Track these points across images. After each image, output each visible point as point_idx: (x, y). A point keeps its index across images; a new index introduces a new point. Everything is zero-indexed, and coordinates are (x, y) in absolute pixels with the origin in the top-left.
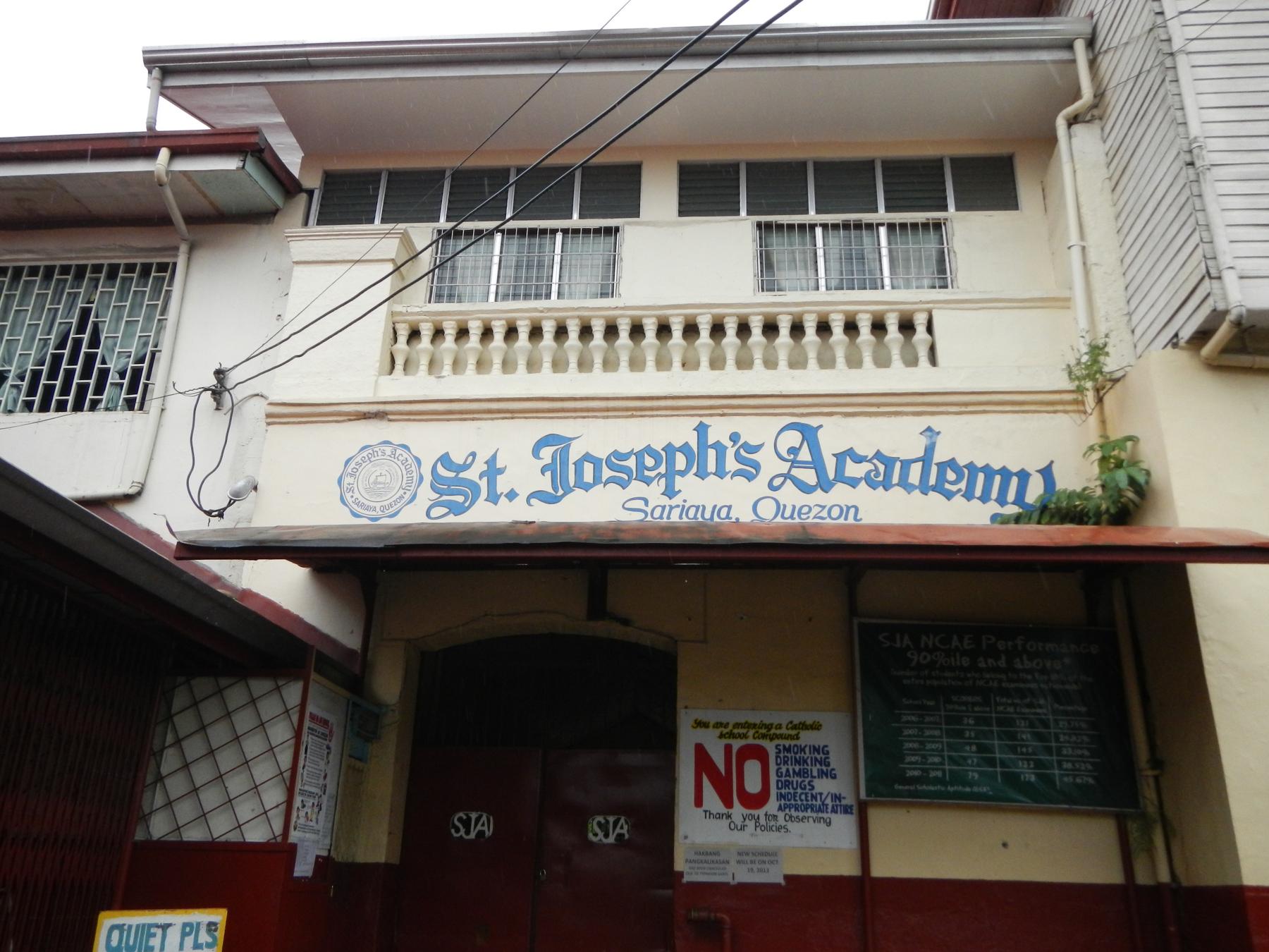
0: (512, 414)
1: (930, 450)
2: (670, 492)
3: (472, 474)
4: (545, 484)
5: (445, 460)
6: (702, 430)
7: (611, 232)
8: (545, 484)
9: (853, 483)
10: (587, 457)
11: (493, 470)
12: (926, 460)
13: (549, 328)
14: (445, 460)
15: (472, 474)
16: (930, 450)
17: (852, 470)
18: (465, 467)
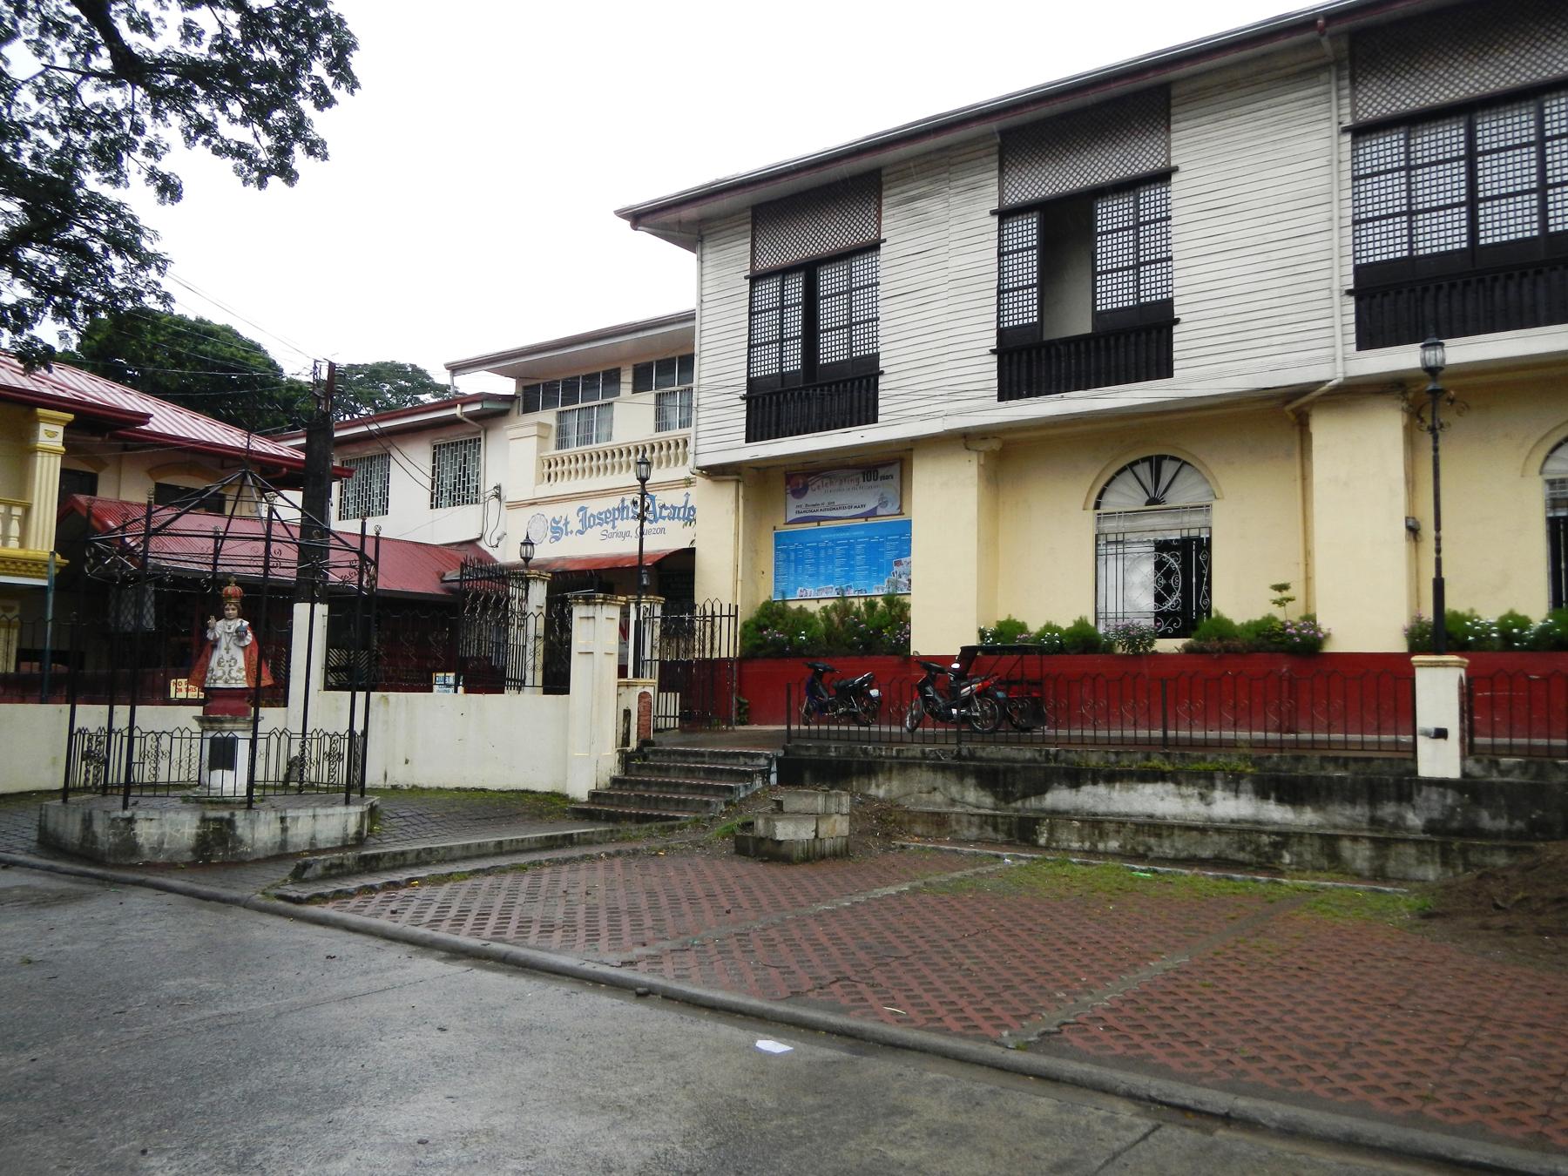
0: (571, 499)
1: (686, 502)
2: (614, 527)
3: (561, 525)
4: (580, 527)
5: (554, 519)
6: (623, 501)
7: (611, 404)
8: (580, 527)
9: (664, 518)
10: (592, 515)
11: (567, 523)
12: (685, 507)
13: (587, 456)
14: (554, 519)
15: (561, 525)
16: (686, 502)
17: (665, 513)
18: (558, 523)
